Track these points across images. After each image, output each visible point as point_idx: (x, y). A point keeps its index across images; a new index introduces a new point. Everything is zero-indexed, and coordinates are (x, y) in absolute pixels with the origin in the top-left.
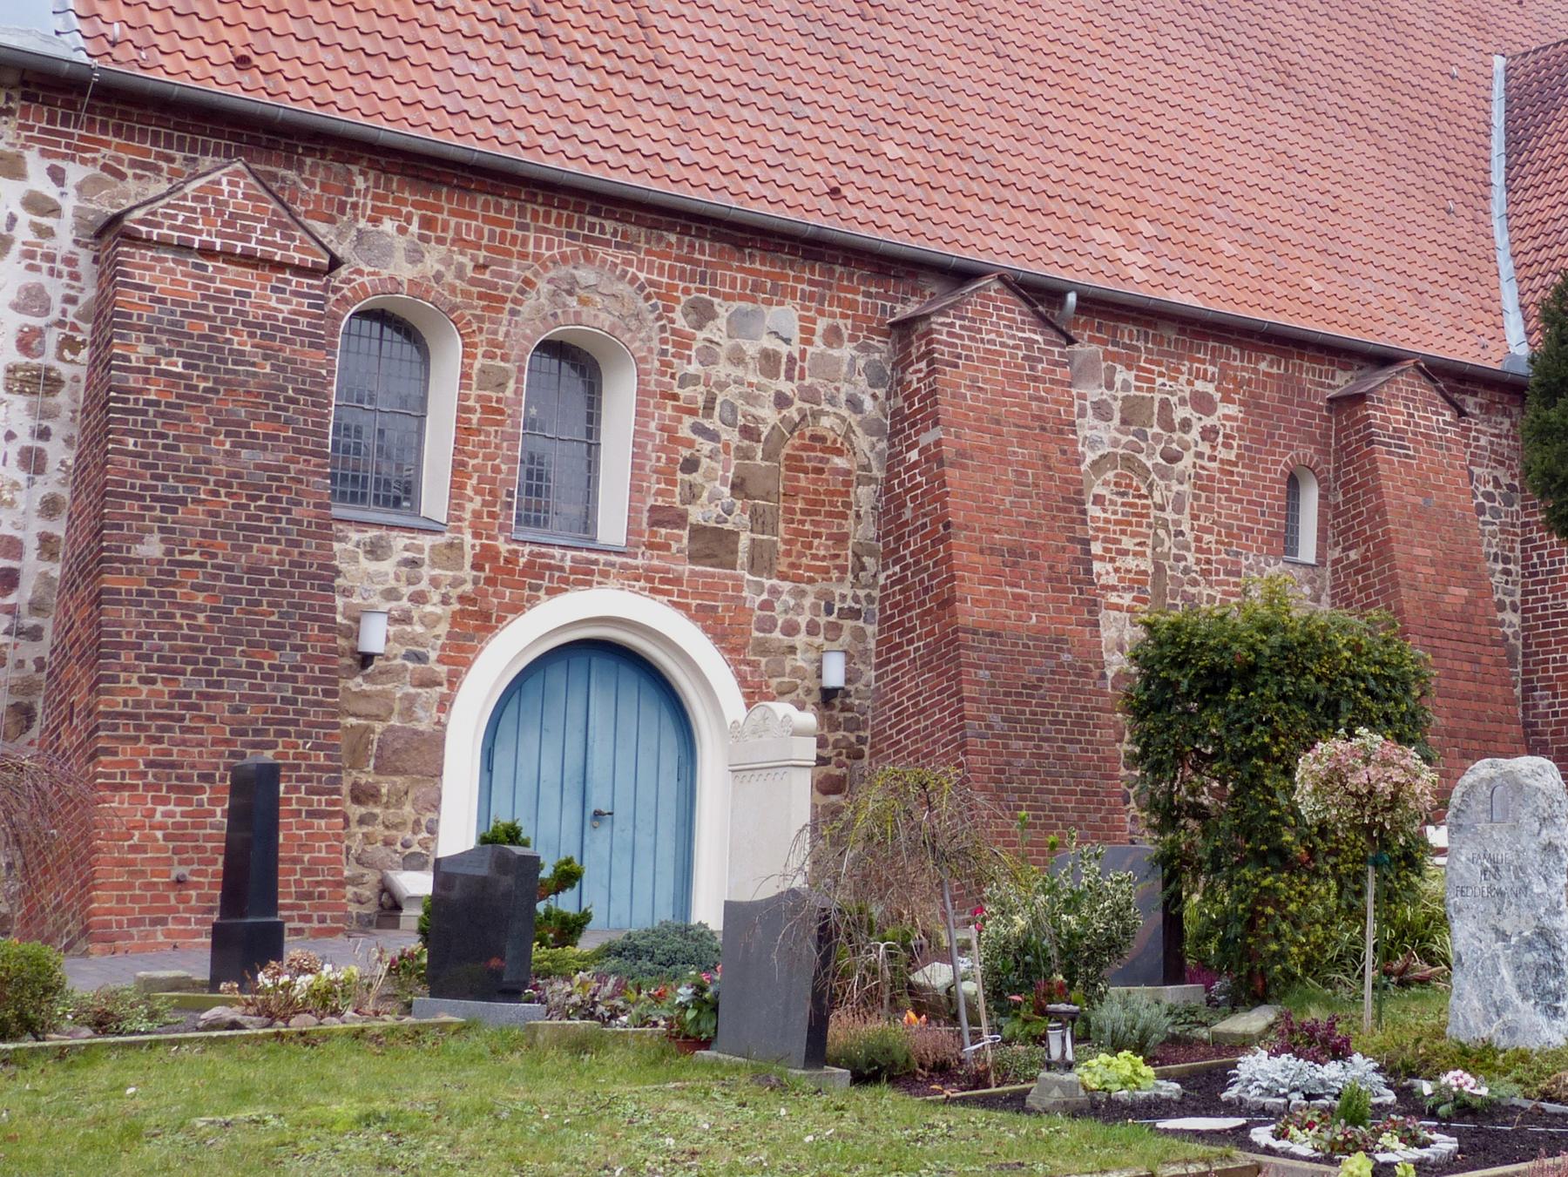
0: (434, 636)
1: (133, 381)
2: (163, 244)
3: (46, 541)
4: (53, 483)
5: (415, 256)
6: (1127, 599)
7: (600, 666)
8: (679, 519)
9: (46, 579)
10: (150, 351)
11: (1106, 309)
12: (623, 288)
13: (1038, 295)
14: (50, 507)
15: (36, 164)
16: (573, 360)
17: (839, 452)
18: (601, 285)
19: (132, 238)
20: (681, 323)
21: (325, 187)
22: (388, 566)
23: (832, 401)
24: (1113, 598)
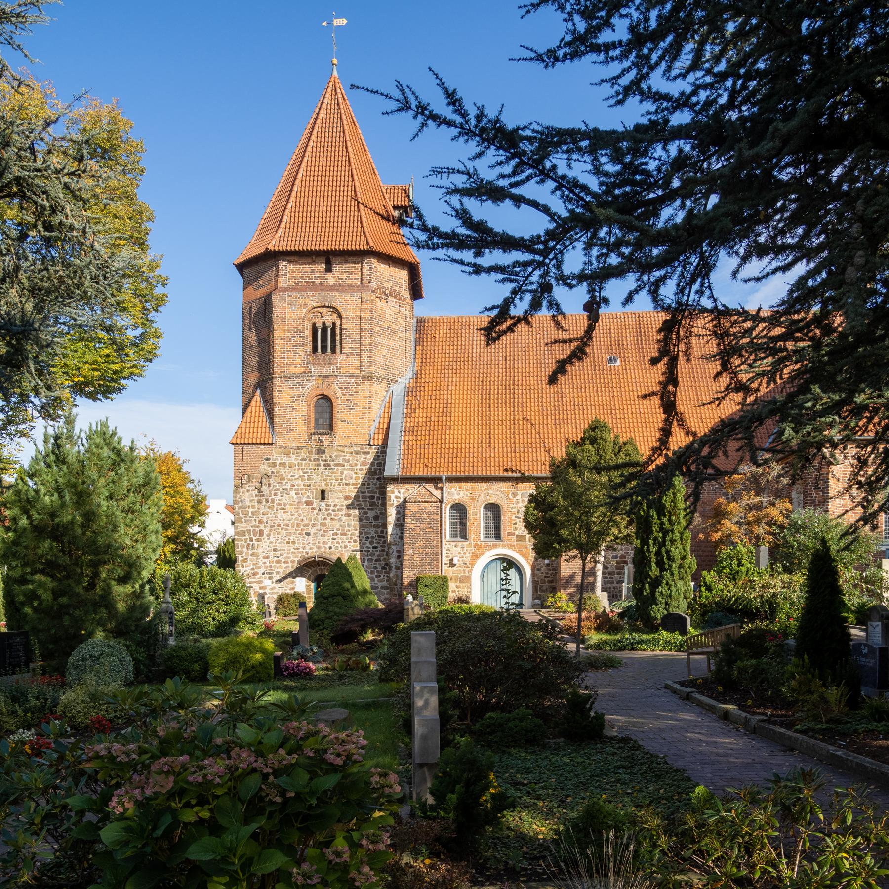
0: (468, 557)
5: (458, 494)
8: (514, 534)
12: (498, 493)
20: (511, 497)
22: (458, 549)
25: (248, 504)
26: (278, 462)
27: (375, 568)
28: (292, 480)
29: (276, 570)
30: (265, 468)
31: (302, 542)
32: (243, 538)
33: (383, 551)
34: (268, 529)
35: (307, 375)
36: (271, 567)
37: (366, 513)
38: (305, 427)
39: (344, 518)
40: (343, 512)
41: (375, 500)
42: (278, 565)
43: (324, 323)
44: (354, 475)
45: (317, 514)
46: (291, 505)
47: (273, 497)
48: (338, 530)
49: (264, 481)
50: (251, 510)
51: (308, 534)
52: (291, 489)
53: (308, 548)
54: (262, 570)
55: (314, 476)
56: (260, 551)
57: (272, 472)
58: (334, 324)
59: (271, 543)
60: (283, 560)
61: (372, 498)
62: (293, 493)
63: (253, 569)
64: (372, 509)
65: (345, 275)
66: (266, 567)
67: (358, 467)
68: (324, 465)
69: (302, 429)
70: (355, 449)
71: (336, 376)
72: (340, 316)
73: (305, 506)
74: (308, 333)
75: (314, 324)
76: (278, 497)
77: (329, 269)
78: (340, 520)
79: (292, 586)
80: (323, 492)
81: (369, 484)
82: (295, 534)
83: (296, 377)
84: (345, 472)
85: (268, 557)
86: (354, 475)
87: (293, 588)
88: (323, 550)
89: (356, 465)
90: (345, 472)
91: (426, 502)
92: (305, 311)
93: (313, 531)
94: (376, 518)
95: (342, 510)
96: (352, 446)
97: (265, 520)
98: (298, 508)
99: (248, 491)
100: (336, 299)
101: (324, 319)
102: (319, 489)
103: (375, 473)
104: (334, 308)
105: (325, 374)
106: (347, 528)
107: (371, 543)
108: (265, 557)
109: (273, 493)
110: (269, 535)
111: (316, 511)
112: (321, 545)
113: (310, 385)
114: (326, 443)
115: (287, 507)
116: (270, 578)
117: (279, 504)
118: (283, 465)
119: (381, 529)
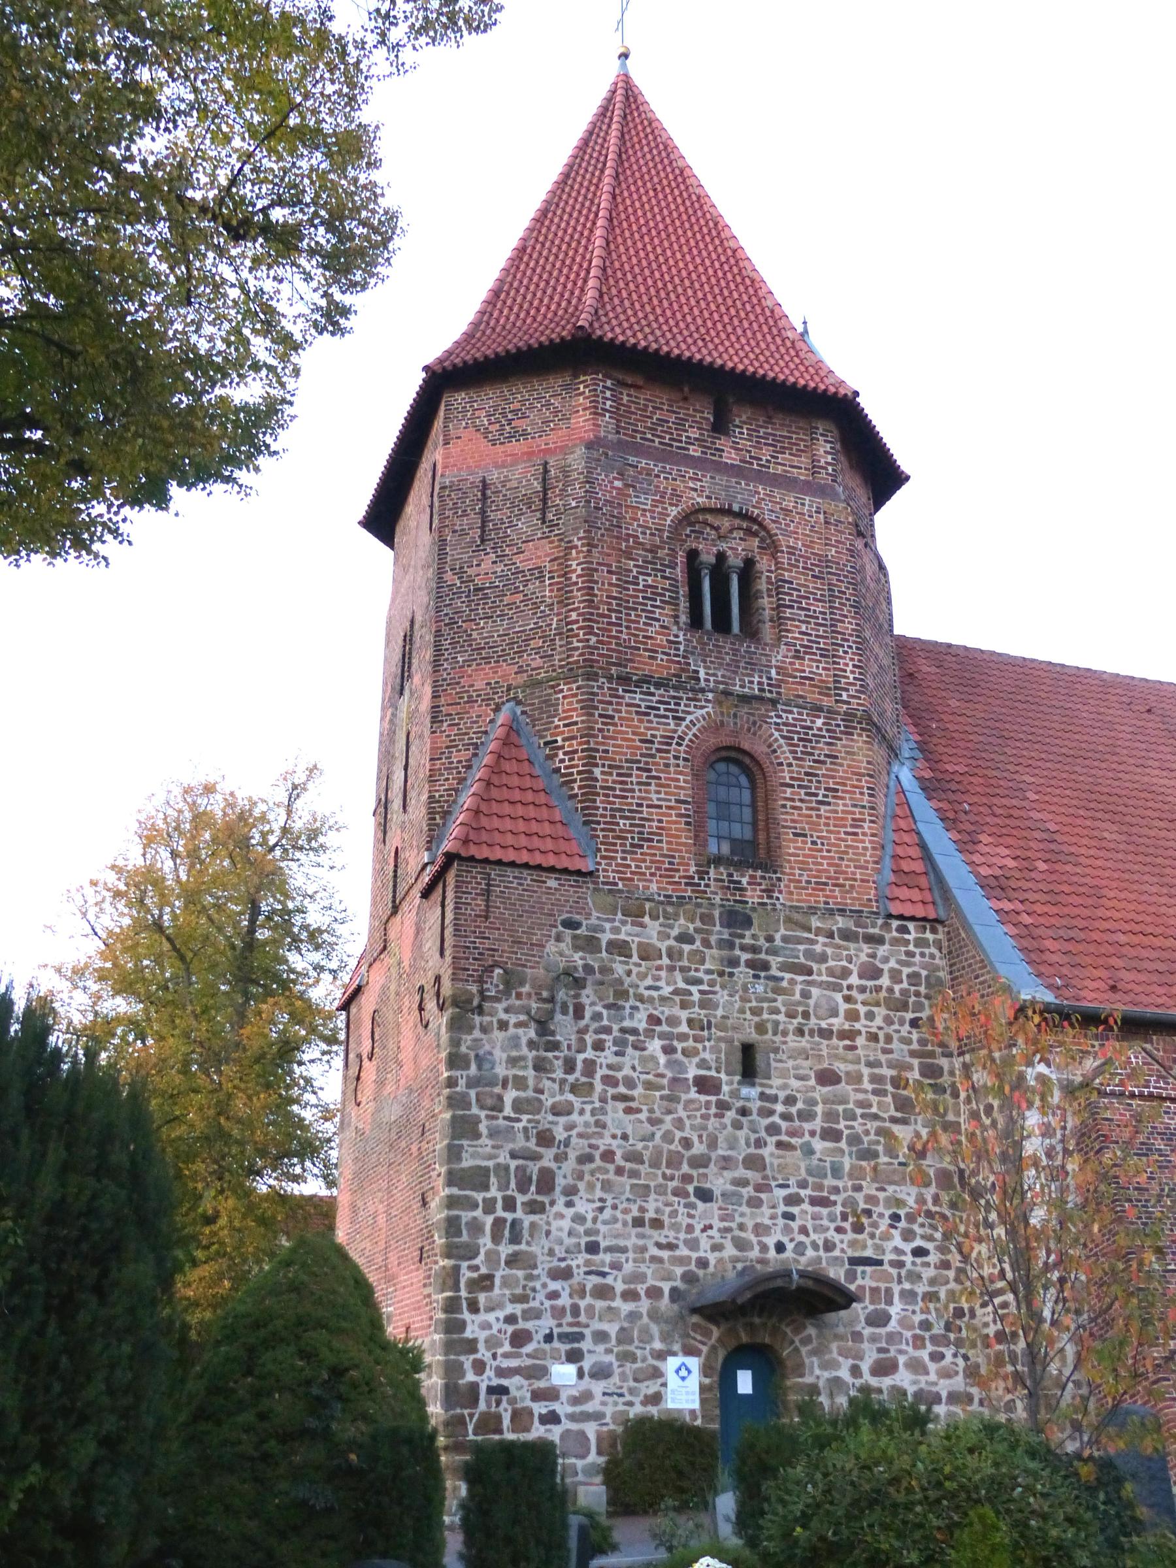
2: (1113, 1094)
21: (1165, 1051)
25: (501, 1071)
26: (605, 938)
27: (926, 1325)
28: (651, 1000)
29: (597, 1325)
30: (561, 952)
31: (684, 1220)
32: (479, 1197)
33: (946, 1265)
34: (570, 1165)
35: (683, 683)
36: (576, 1311)
39: (819, 1145)
40: (818, 1124)
42: (600, 1304)
43: (721, 557)
45: (737, 1125)
46: (649, 1086)
47: (589, 1054)
48: (803, 1185)
49: (561, 995)
50: (510, 1096)
51: (705, 1195)
52: (650, 1033)
53: (705, 1244)
54: (547, 1323)
55: (722, 997)
57: (588, 969)
58: (749, 563)
59: (579, 1219)
60: (620, 1287)
62: (655, 1046)
63: (511, 1319)
64: (904, 1122)
65: (766, 454)
66: (559, 1313)
68: (750, 964)
70: (841, 922)
72: (771, 546)
73: (693, 1094)
74: (679, 572)
75: (693, 555)
76: (607, 1057)
77: (720, 426)
78: (809, 1151)
79: (651, 1387)
80: (748, 1050)
81: (889, 1039)
82: (661, 1190)
83: (658, 685)
84: (815, 992)
85: (564, 1274)
86: (843, 1007)
87: (656, 1399)
88: (755, 1253)
89: (846, 973)
90: (815, 992)
92: (673, 512)
93: (719, 1183)
96: (831, 912)
97: (560, 1134)
98: (672, 1099)
99: (503, 1025)
100: (761, 500)
101: (723, 546)
102: (738, 1038)
103: (904, 1007)
104: (754, 520)
106: (829, 1182)
107: (908, 1236)
108: (555, 1274)
109: (589, 1038)
110: (570, 1191)
111: (731, 1115)
113: (699, 714)
114: (753, 897)
115: (638, 1092)
116: (574, 1357)
118: (620, 948)
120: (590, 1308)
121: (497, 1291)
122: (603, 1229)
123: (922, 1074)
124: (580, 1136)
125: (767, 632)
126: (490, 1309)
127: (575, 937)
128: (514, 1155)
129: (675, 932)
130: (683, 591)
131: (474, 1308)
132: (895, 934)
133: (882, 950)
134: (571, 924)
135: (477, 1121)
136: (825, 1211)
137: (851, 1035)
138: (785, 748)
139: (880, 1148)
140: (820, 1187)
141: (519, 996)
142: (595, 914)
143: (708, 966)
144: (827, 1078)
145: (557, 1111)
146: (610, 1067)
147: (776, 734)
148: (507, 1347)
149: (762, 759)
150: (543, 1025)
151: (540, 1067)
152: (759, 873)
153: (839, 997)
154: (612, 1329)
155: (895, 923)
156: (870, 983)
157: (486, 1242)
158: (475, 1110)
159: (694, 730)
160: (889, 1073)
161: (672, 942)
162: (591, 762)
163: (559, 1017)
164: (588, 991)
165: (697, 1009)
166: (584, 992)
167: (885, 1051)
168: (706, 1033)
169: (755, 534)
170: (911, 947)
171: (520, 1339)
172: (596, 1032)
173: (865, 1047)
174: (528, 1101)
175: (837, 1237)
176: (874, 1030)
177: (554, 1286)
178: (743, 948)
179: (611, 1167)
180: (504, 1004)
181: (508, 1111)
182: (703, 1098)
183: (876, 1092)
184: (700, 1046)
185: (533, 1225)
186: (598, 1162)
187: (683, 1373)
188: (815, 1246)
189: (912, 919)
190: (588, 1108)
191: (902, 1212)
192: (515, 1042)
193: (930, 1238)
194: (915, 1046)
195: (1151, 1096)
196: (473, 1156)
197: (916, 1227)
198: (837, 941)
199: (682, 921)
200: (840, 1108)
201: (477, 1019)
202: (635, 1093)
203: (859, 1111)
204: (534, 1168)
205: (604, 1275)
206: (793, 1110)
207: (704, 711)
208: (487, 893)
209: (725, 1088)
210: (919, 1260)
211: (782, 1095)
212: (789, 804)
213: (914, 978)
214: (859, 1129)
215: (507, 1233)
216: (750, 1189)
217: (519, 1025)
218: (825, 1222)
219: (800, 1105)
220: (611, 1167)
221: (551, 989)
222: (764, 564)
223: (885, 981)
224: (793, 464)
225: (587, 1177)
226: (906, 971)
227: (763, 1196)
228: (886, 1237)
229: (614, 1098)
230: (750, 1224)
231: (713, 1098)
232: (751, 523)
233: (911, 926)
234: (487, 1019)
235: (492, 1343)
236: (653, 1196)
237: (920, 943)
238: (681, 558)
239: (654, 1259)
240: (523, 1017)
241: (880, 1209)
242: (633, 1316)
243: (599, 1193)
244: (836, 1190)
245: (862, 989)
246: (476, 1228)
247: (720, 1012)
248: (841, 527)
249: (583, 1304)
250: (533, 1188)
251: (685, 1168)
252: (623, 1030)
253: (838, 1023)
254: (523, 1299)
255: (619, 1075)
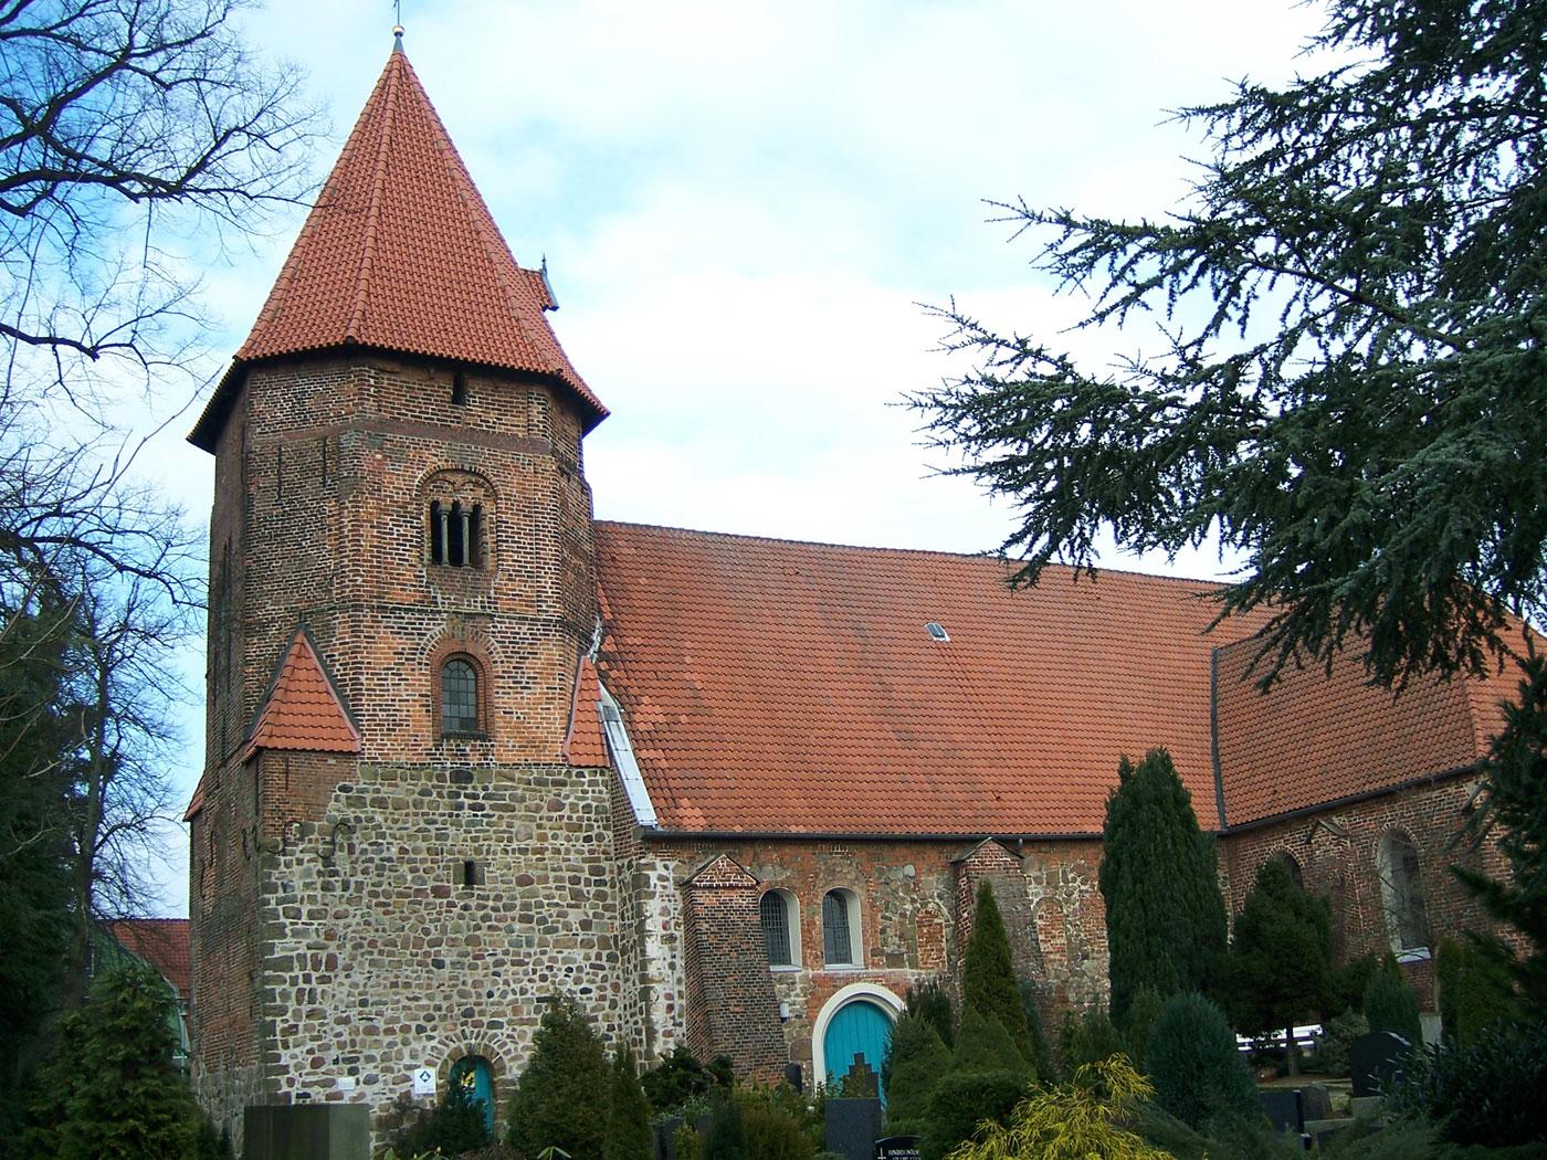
1: (705, 937)
2: (705, 887)
3: (680, 992)
4: (680, 973)
6: (1058, 957)
7: (862, 1009)
9: (681, 1006)
10: (707, 926)
11: (1035, 842)
13: (1008, 843)
14: (679, 981)
15: (659, 864)
16: (838, 898)
17: (937, 917)
18: (846, 871)
19: (695, 887)
23: (932, 897)
24: (1052, 957)
26: (368, 797)
29: (367, 1052)
30: (336, 809)
32: (287, 975)
33: (603, 998)
35: (427, 607)
36: (353, 1043)
37: (565, 915)
38: (427, 722)
39: (517, 926)
40: (516, 913)
41: (581, 886)
43: (456, 505)
44: (536, 832)
46: (400, 895)
48: (506, 953)
49: (339, 839)
51: (439, 965)
52: (401, 860)
54: (334, 1053)
55: (452, 831)
56: (327, 1006)
57: (358, 819)
58: (477, 508)
59: (354, 985)
61: (575, 881)
62: (405, 868)
63: (311, 1051)
64: (577, 906)
65: (492, 417)
66: (342, 1046)
67: (544, 813)
68: (472, 807)
69: (420, 725)
71: (492, 617)
72: (493, 495)
75: (435, 505)
77: (458, 398)
81: (568, 851)
83: (407, 611)
84: (517, 823)
85: (346, 1021)
86: (536, 832)
89: (538, 809)
90: (517, 823)
91: (731, 887)
94: (586, 925)
95: (513, 907)
99: (300, 862)
100: (485, 459)
101: (458, 497)
104: (481, 476)
105: (465, 609)
106: (524, 950)
107: (577, 981)
108: (339, 1021)
110: (348, 968)
112: (468, 987)
113: (437, 629)
114: (474, 760)
117: (374, 894)
119: (596, 949)
120: (363, 1042)
121: (300, 1035)
122: (371, 991)
123: (591, 874)
124: (354, 932)
125: (490, 561)
126: (295, 1046)
127: (348, 798)
128: (309, 948)
129: (417, 790)
130: (427, 534)
131: (286, 1046)
132: (574, 778)
133: (565, 790)
134: (344, 789)
135: (285, 926)
136: (521, 969)
137: (541, 851)
138: (500, 650)
139: (560, 926)
140: (518, 954)
141: (310, 841)
142: (362, 781)
143: (441, 811)
144: (524, 881)
145: (337, 916)
146: (373, 885)
147: (493, 640)
148: (308, 1069)
149: (482, 659)
150: (327, 859)
151: (327, 887)
152: (479, 742)
153: (534, 825)
154: (377, 1053)
155: (575, 771)
156: (555, 814)
157: (292, 1005)
158: (282, 920)
159: (433, 642)
160: (567, 874)
161: (416, 796)
162: (358, 671)
163: (338, 853)
164: (358, 834)
165: (433, 841)
166: (354, 836)
167: (564, 860)
168: (439, 857)
169: (482, 486)
170: (586, 787)
171: (317, 1063)
172: (363, 862)
173: (550, 859)
174: (319, 911)
175: (529, 985)
176: (558, 846)
177: (339, 1029)
178: (466, 796)
179: (376, 951)
180: (301, 847)
181: (304, 919)
182: (438, 901)
183: (557, 888)
184: (435, 866)
185: (323, 991)
186: (366, 948)
187: (425, 1077)
188: (514, 992)
189: (587, 767)
190: (359, 912)
191: (574, 966)
192: (307, 873)
193: (593, 982)
194: (587, 855)
195: (731, 887)
196: (283, 949)
197: (583, 975)
198: (533, 786)
199: (423, 781)
200: (533, 901)
201: (282, 858)
202: (391, 901)
203: (546, 902)
204: (323, 955)
205: (371, 1019)
206: (500, 904)
207: (440, 628)
208: (287, 772)
209: (453, 894)
210: (584, 996)
211: (492, 895)
212: (501, 691)
213: (587, 808)
214: (545, 914)
215: (306, 997)
216: (470, 958)
217: (310, 861)
218: (521, 976)
219: (505, 900)
220: (376, 951)
221: (333, 835)
222: (488, 508)
223: (566, 812)
224: (513, 424)
225: (359, 958)
226: (582, 804)
227: (479, 962)
228: (562, 983)
229: (377, 905)
230: (470, 981)
231: (445, 901)
232: (479, 478)
233: (586, 772)
234: (288, 858)
235: (299, 1067)
236: (404, 967)
237: (591, 783)
238: (426, 509)
239: (404, 1007)
240: (313, 856)
241: (559, 965)
242: (391, 1045)
243: (367, 968)
244: (529, 955)
245: (550, 819)
246: (285, 996)
247: (449, 842)
248: (547, 475)
249: (358, 1039)
250: (323, 968)
251: (426, 948)
252: (382, 860)
253: (534, 843)
254: (318, 1038)
255: (380, 889)
